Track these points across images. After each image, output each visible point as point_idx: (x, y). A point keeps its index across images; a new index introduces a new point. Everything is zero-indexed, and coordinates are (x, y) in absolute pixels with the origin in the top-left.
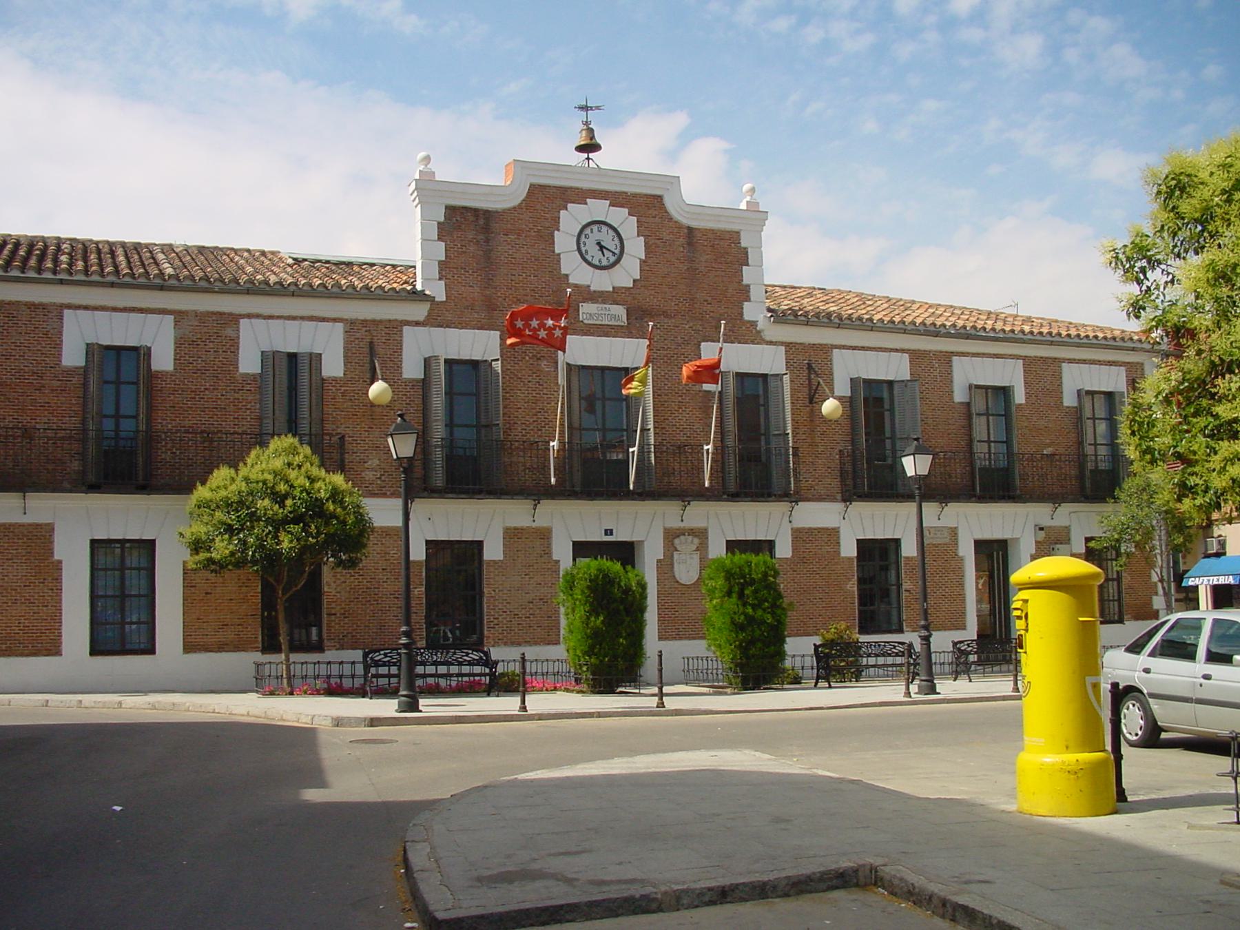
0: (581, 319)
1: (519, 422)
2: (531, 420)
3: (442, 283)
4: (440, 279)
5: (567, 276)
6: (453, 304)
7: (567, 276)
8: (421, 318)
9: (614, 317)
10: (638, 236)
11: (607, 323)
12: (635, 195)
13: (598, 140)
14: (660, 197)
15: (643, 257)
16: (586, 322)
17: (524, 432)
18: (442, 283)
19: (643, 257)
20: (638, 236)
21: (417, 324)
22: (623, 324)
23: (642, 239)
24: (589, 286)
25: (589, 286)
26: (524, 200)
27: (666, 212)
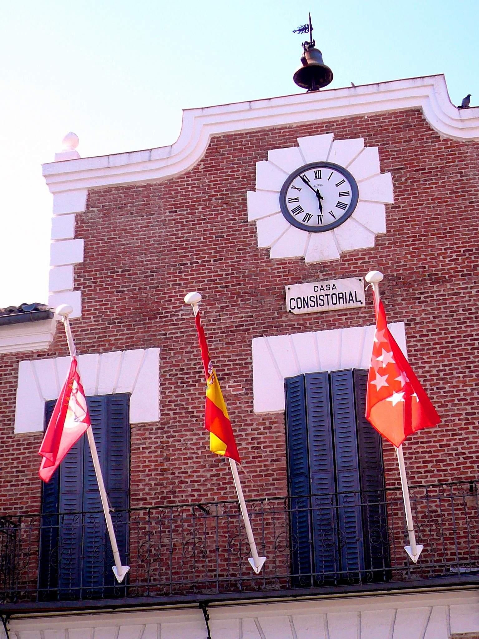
0: (288, 309)
1: (188, 480)
2: (208, 475)
3: (79, 292)
4: (76, 289)
5: (267, 251)
6: (93, 320)
7: (267, 251)
8: (45, 347)
9: (341, 296)
10: (382, 171)
11: (332, 307)
12: (375, 118)
13: (327, 61)
14: (418, 112)
15: (391, 201)
16: (296, 311)
17: (196, 494)
18: (79, 292)
19: (391, 201)
20: (382, 171)
21: (41, 355)
22: (359, 305)
23: (388, 176)
24: (302, 259)
25: (302, 259)
26: (202, 161)
27: (429, 129)
